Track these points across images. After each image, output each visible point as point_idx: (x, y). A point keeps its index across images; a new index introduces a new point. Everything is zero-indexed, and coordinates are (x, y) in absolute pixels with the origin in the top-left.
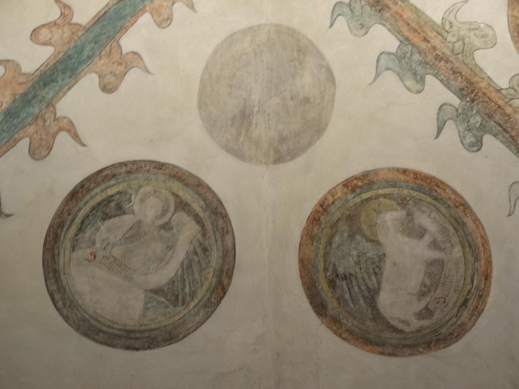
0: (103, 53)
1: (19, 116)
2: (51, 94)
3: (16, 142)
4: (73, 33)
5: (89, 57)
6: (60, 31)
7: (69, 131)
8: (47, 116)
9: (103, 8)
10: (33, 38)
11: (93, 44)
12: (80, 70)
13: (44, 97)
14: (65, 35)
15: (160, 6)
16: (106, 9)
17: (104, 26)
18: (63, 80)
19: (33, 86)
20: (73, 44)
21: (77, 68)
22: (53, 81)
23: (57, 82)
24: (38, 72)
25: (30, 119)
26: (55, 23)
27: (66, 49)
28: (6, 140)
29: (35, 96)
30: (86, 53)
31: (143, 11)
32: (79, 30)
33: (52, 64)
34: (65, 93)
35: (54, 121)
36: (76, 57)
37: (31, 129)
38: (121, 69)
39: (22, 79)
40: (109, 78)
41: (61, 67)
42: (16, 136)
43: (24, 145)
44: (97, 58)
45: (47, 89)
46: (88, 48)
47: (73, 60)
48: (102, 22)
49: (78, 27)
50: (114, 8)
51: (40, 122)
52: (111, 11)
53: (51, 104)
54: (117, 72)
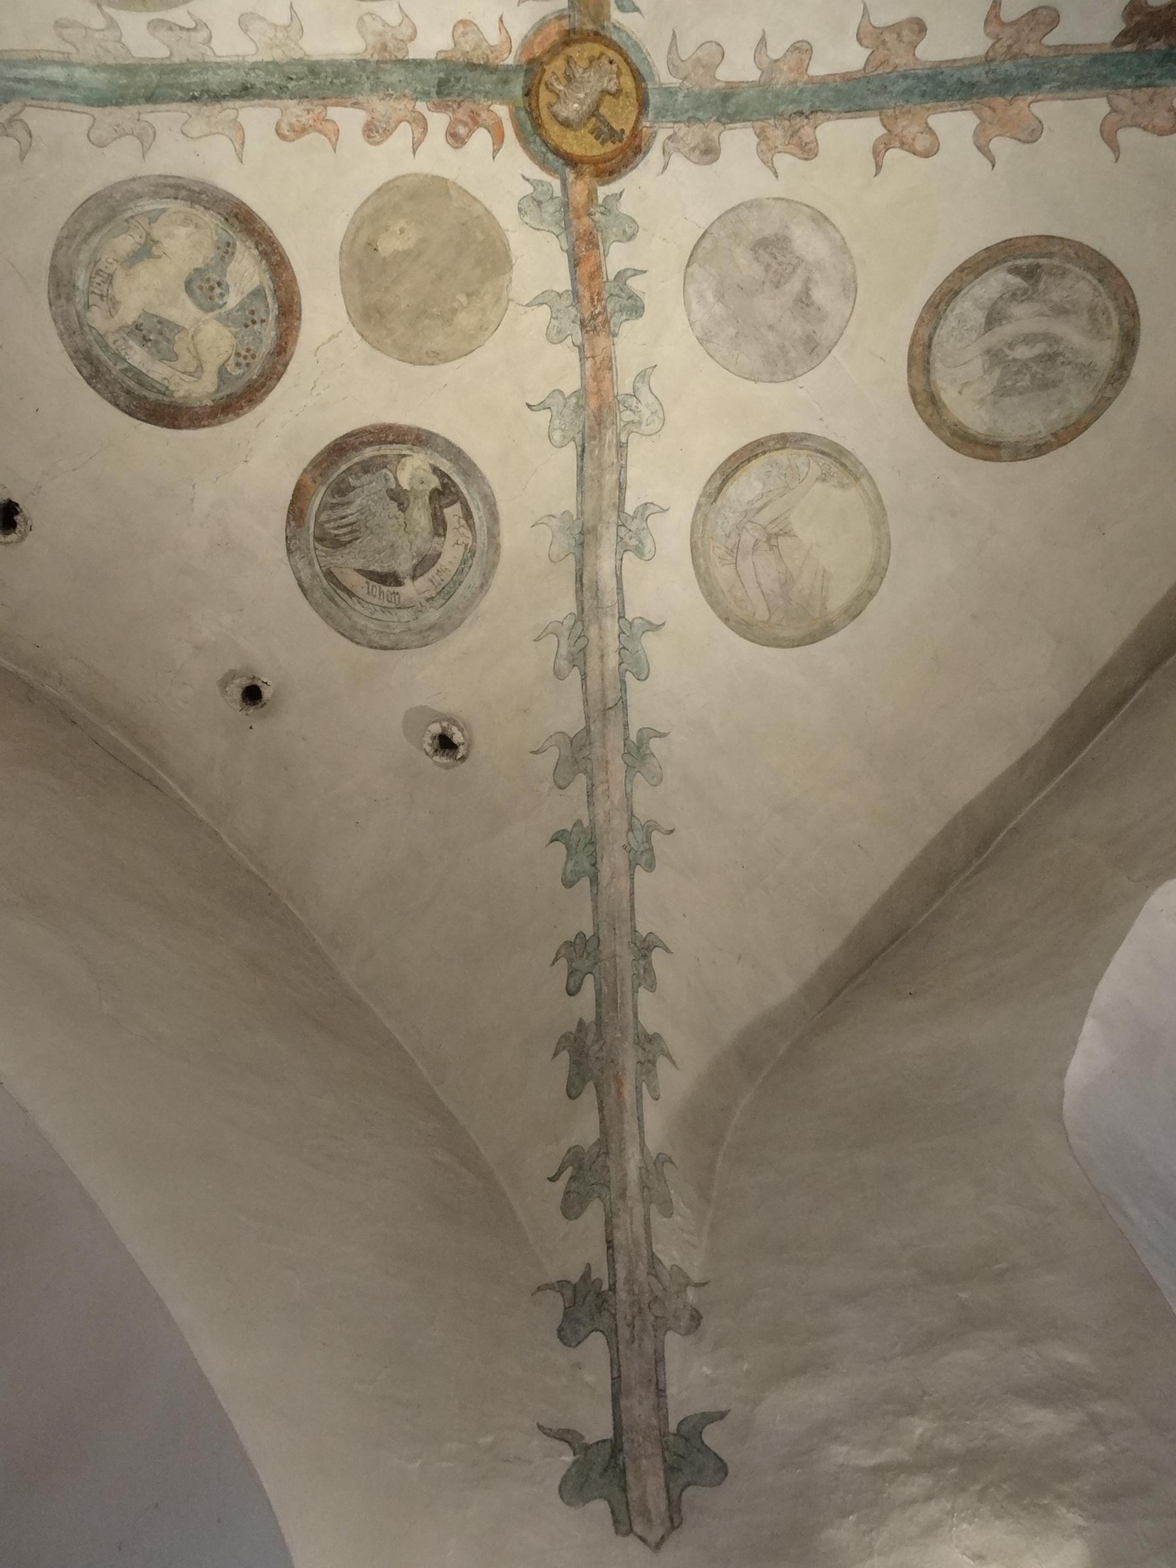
0: (888, 70)
1: (1029, 74)
2: (976, 71)
3: (1057, 48)
4: (896, 118)
5: (905, 77)
6: (905, 132)
7: (997, 16)
8: (1004, 50)
9: (845, 118)
10: (935, 149)
11: (890, 88)
12: (926, 72)
13: (987, 73)
14: (905, 123)
15: (791, 70)
16: (843, 115)
17: (862, 99)
18: (952, 76)
19: (985, 94)
20: (906, 106)
21: (928, 76)
22: (963, 83)
23: (959, 79)
24: (966, 106)
25: (1021, 61)
26: (902, 145)
27: (918, 107)
28: (1065, 58)
29: (994, 82)
30: (904, 84)
31: (811, 80)
32: (888, 118)
33: (946, 103)
34: (962, 59)
35: (1000, 39)
36: (917, 90)
37: (1031, 49)
38: (888, 37)
39: (987, 113)
40: (907, 35)
41: (941, 91)
42: (1052, 54)
43: (1053, 39)
44: (899, 69)
45: (975, 79)
46: (897, 89)
47: (924, 88)
48: (860, 105)
49: (885, 121)
50: (835, 110)
51: (1015, 49)
52: (840, 109)
53: (988, 60)
54: (895, 36)
